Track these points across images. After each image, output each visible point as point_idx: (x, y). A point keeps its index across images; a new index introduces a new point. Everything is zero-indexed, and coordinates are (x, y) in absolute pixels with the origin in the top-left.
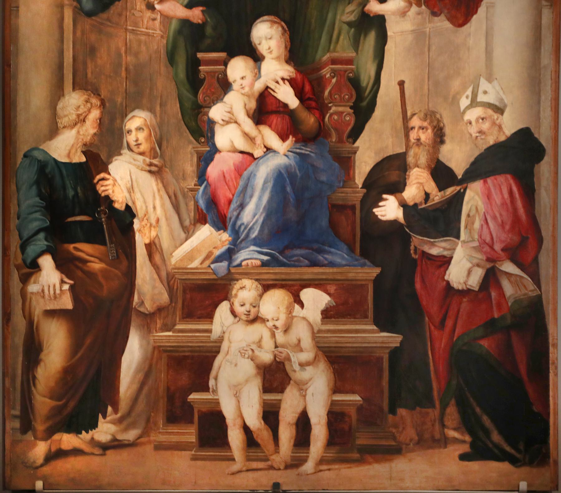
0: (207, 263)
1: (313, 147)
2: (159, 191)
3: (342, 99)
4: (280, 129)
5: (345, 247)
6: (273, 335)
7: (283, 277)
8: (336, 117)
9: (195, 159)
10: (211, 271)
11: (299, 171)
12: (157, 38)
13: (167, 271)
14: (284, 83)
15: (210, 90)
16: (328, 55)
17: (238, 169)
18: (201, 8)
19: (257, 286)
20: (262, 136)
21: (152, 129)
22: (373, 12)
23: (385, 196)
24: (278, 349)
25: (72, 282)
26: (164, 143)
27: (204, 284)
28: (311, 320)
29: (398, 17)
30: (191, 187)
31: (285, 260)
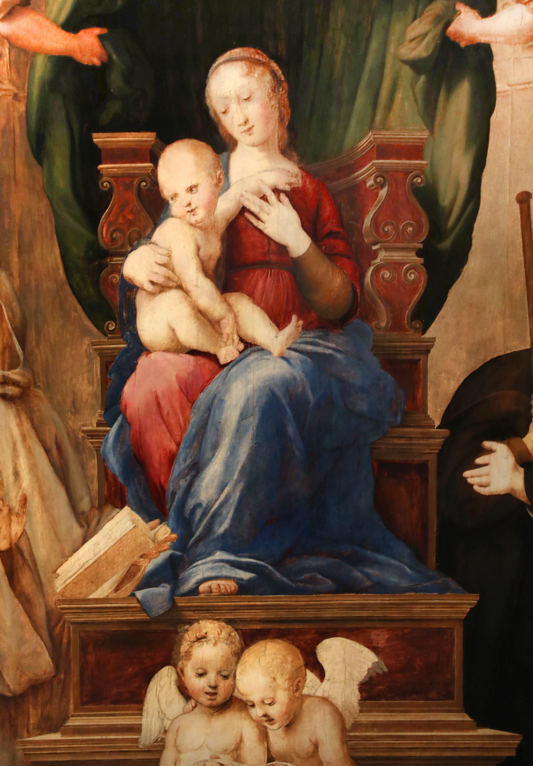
0: (129, 587)
1: (341, 339)
2: (24, 437)
3: (400, 235)
4: (271, 301)
5: (407, 552)
6: (264, 735)
7: (283, 614)
8: (387, 274)
9: (97, 368)
10: (138, 605)
11: (312, 391)
12: (6, 101)
13: (46, 606)
14: (280, 201)
15: (124, 217)
16: (370, 137)
17: (186, 389)
18: (97, 31)
19: (230, 635)
20: (236, 317)
21: (5, 304)
22: (466, 37)
23: (487, 444)
24: (274, 763)
26: (32, 335)
27: (124, 631)
28: (339, 701)
29: (519, 47)
30: (90, 428)
31: (285, 579)
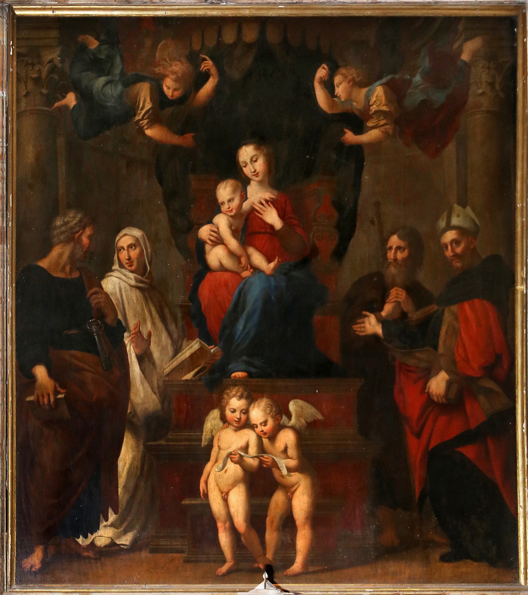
25: (65, 391)
